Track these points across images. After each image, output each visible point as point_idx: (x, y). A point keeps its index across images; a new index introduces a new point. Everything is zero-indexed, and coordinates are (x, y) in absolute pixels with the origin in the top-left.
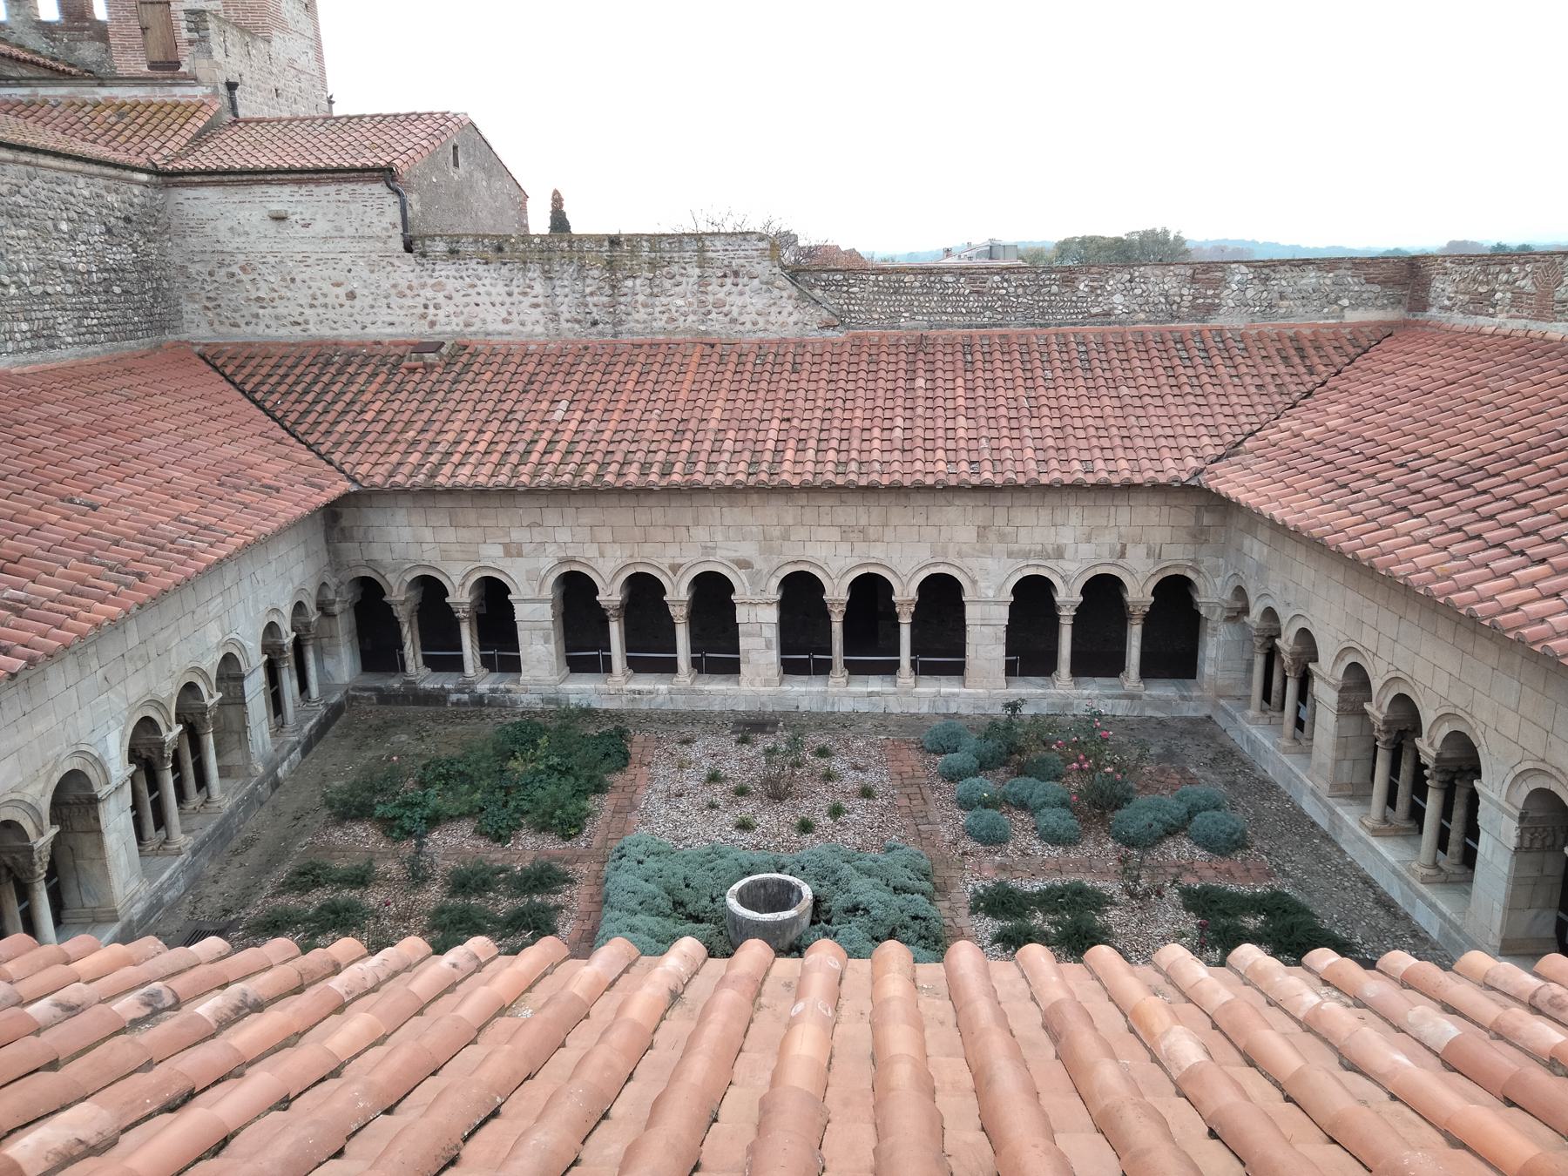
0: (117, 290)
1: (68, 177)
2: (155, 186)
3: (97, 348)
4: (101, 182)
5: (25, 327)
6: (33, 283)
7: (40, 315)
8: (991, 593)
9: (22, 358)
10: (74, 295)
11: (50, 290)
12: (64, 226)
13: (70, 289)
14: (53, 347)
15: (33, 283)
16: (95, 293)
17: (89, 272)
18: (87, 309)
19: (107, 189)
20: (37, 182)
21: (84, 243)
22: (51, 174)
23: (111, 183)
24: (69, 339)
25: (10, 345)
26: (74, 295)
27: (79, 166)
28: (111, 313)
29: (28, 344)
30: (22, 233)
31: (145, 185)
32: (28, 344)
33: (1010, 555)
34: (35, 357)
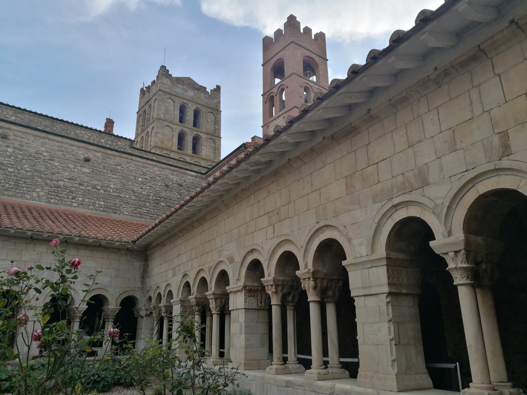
0: (162, 204)
1: (151, 167)
2: (202, 178)
3: (143, 220)
4: (168, 171)
5: (102, 203)
6: (113, 192)
7: (111, 201)
8: (364, 251)
9: (95, 212)
10: (136, 200)
11: (121, 195)
12: (140, 180)
13: (134, 198)
14: (115, 213)
15: (113, 192)
16: (149, 202)
17: (147, 195)
18: (141, 207)
19: (172, 174)
20: (131, 165)
21: (149, 186)
22: (139, 163)
23: (175, 173)
24: (127, 213)
25: (91, 207)
26: (136, 200)
27: (154, 163)
28: (156, 211)
29: (102, 209)
30: (113, 176)
31: (195, 177)
32: (102, 209)
33: (375, 199)
34: (102, 213)
